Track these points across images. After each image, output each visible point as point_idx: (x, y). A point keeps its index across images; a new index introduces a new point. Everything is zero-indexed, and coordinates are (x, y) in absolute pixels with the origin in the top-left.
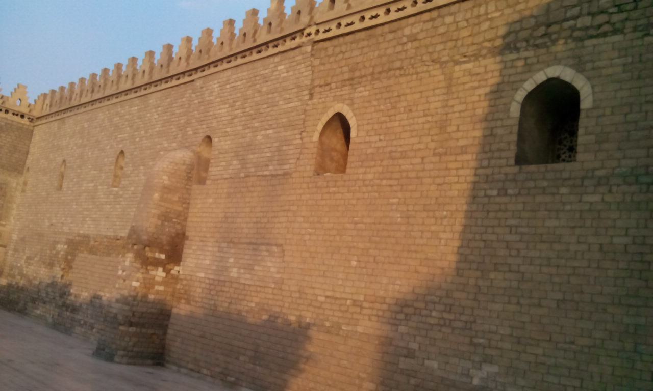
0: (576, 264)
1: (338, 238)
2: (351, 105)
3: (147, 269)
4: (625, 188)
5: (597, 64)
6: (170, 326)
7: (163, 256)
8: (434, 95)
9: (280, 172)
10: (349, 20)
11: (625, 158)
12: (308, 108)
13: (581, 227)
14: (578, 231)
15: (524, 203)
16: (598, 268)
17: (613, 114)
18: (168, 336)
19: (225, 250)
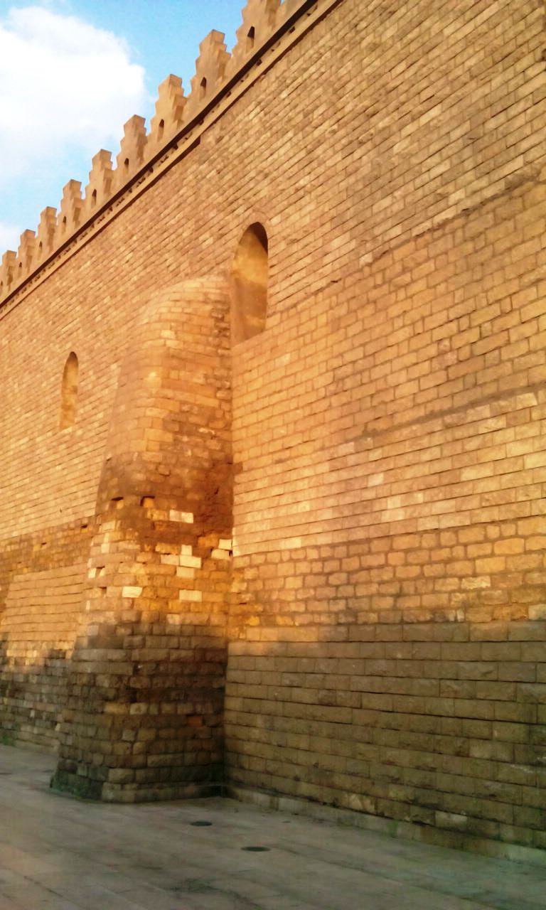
3: (154, 551)
6: (229, 690)
7: (188, 518)
18: (230, 716)
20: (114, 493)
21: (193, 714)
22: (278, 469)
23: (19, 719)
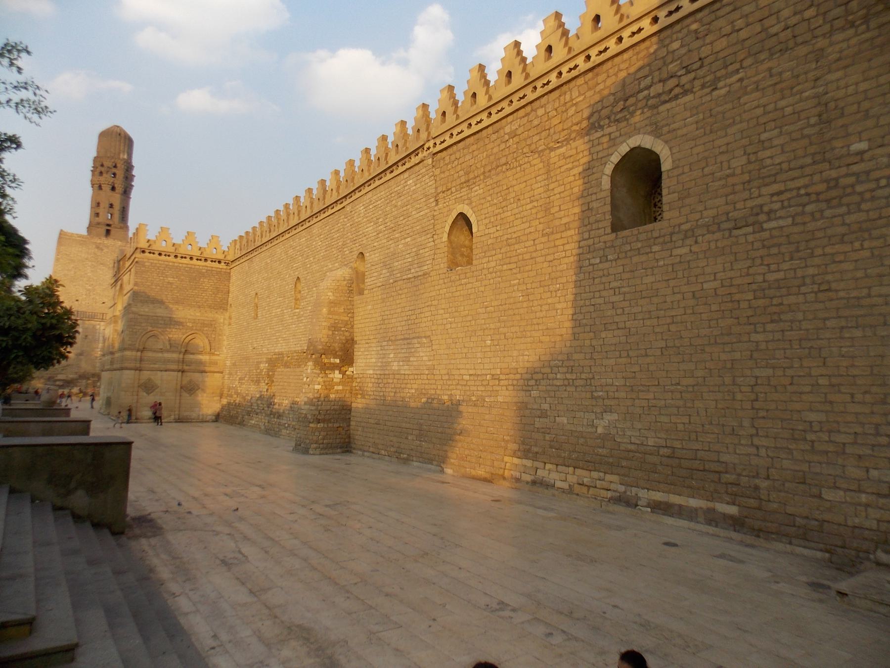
0: (674, 313)
1: (473, 322)
2: (469, 204)
4: (708, 237)
5: (673, 126)
7: (338, 361)
8: (536, 183)
9: (420, 274)
10: (458, 129)
11: (706, 209)
12: (435, 213)
13: (674, 279)
14: (672, 283)
15: (623, 265)
16: (693, 313)
17: (691, 170)
18: (352, 427)
19: (386, 348)
20: (312, 352)
21: (340, 427)
22: (367, 345)
23: (281, 427)
